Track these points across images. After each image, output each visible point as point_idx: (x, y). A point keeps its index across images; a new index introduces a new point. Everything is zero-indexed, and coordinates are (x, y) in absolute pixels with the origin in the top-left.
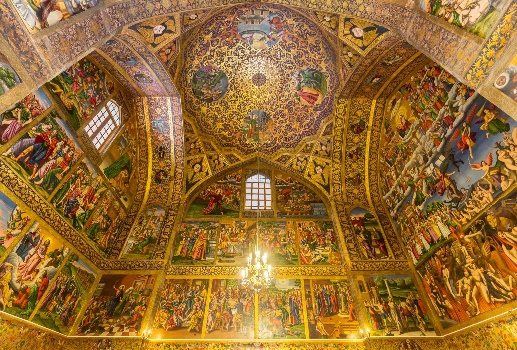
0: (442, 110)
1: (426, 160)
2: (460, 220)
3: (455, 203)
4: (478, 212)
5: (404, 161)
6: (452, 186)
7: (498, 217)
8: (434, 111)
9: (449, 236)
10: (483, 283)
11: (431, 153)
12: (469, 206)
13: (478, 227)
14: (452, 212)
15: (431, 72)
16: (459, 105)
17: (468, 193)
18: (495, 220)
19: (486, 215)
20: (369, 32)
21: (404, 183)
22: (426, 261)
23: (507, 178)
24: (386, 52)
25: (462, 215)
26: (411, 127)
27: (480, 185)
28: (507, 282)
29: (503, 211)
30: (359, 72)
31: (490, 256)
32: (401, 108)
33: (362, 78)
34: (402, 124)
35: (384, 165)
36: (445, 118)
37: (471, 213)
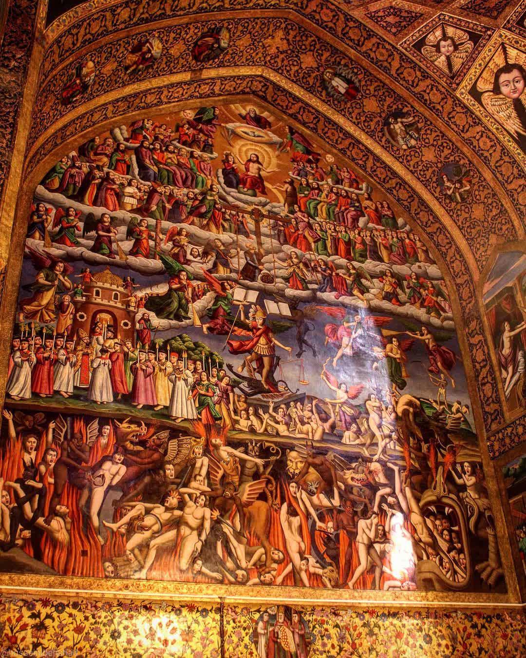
0: (343, 261)
1: (249, 272)
2: (237, 418)
3: (249, 386)
4: (281, 434)
5: (190, 213)
6: (266, 360)
7: (309, 465)
8: (329, 244)
9: (185, 420)
10: (199, 535)
11: (268, 279)
12: (274, 414)
13: (264, 452)
14: (231, 395)
15: (367, 203)
16: (372, 291)
17: (289, 396)
18: (300, 465)
19: (292, 449)
20: (514, 114)
21: (152, 243)
22: (65, 416)
23: (358, 433)
24: (450, 135)
25: (248, 414)
26: (263, 199)
27: (317, 406)
28: (249, 555)
29: (322, 464)
30: (396, 64)
31: (249, 504)
32: (268, 149)
33: (365, 62)
34: (247, 170)
35: (117, 150)
36: (337, 274)
37: (268, 425)
